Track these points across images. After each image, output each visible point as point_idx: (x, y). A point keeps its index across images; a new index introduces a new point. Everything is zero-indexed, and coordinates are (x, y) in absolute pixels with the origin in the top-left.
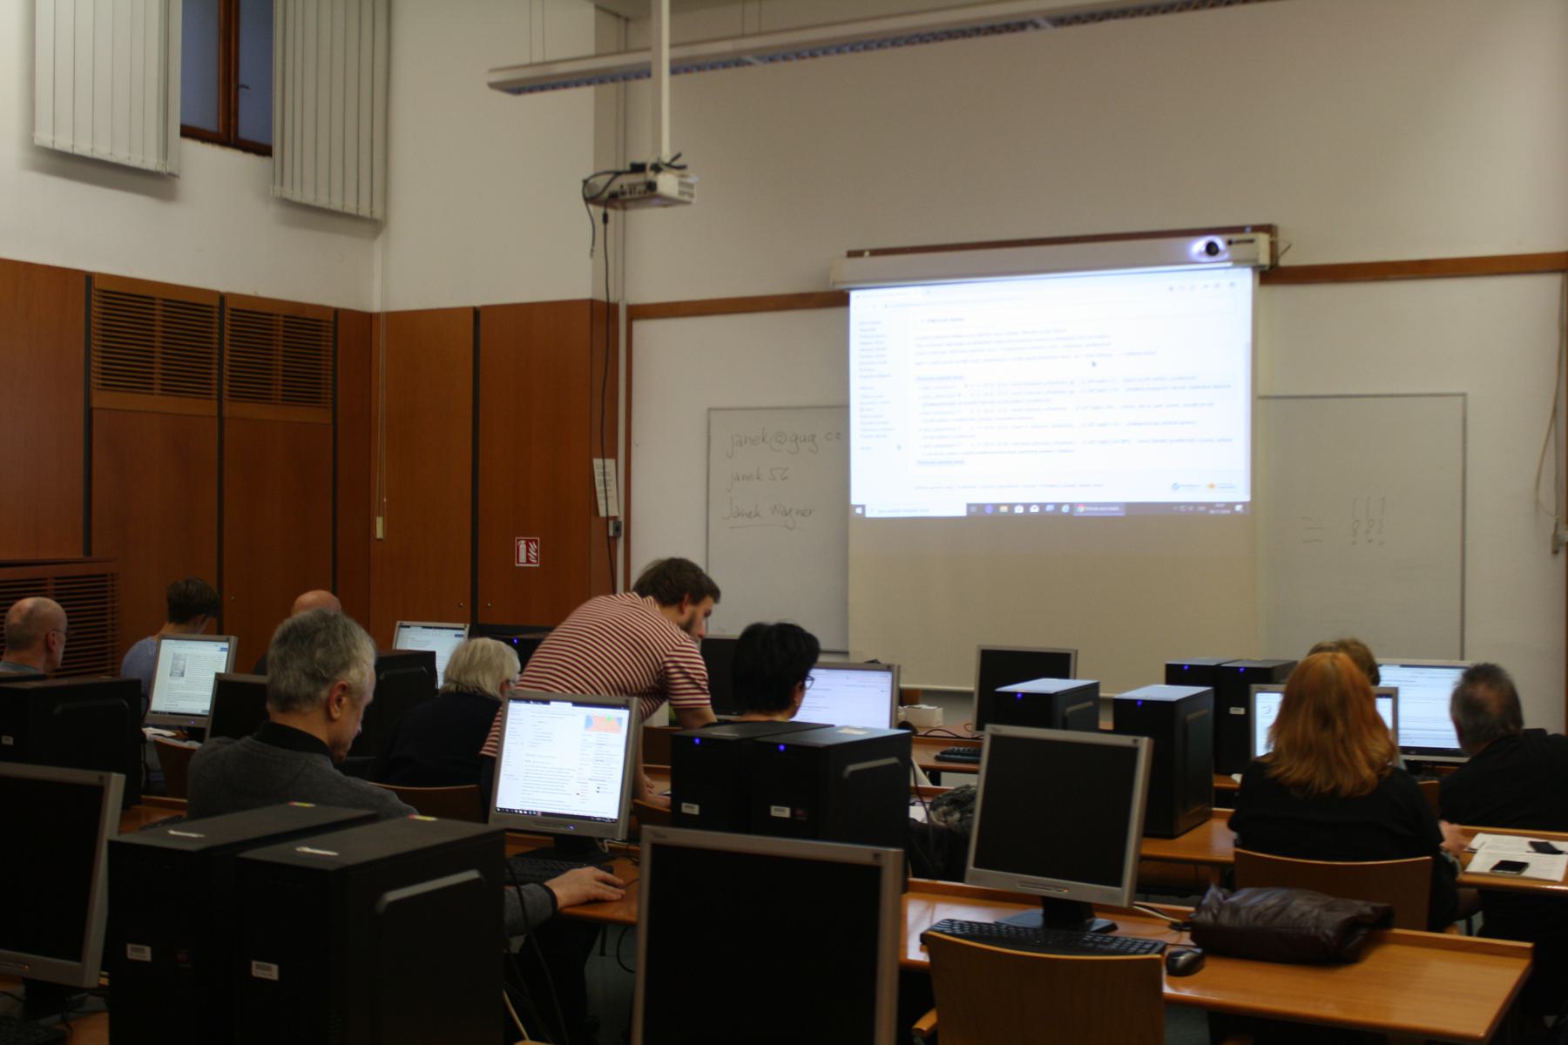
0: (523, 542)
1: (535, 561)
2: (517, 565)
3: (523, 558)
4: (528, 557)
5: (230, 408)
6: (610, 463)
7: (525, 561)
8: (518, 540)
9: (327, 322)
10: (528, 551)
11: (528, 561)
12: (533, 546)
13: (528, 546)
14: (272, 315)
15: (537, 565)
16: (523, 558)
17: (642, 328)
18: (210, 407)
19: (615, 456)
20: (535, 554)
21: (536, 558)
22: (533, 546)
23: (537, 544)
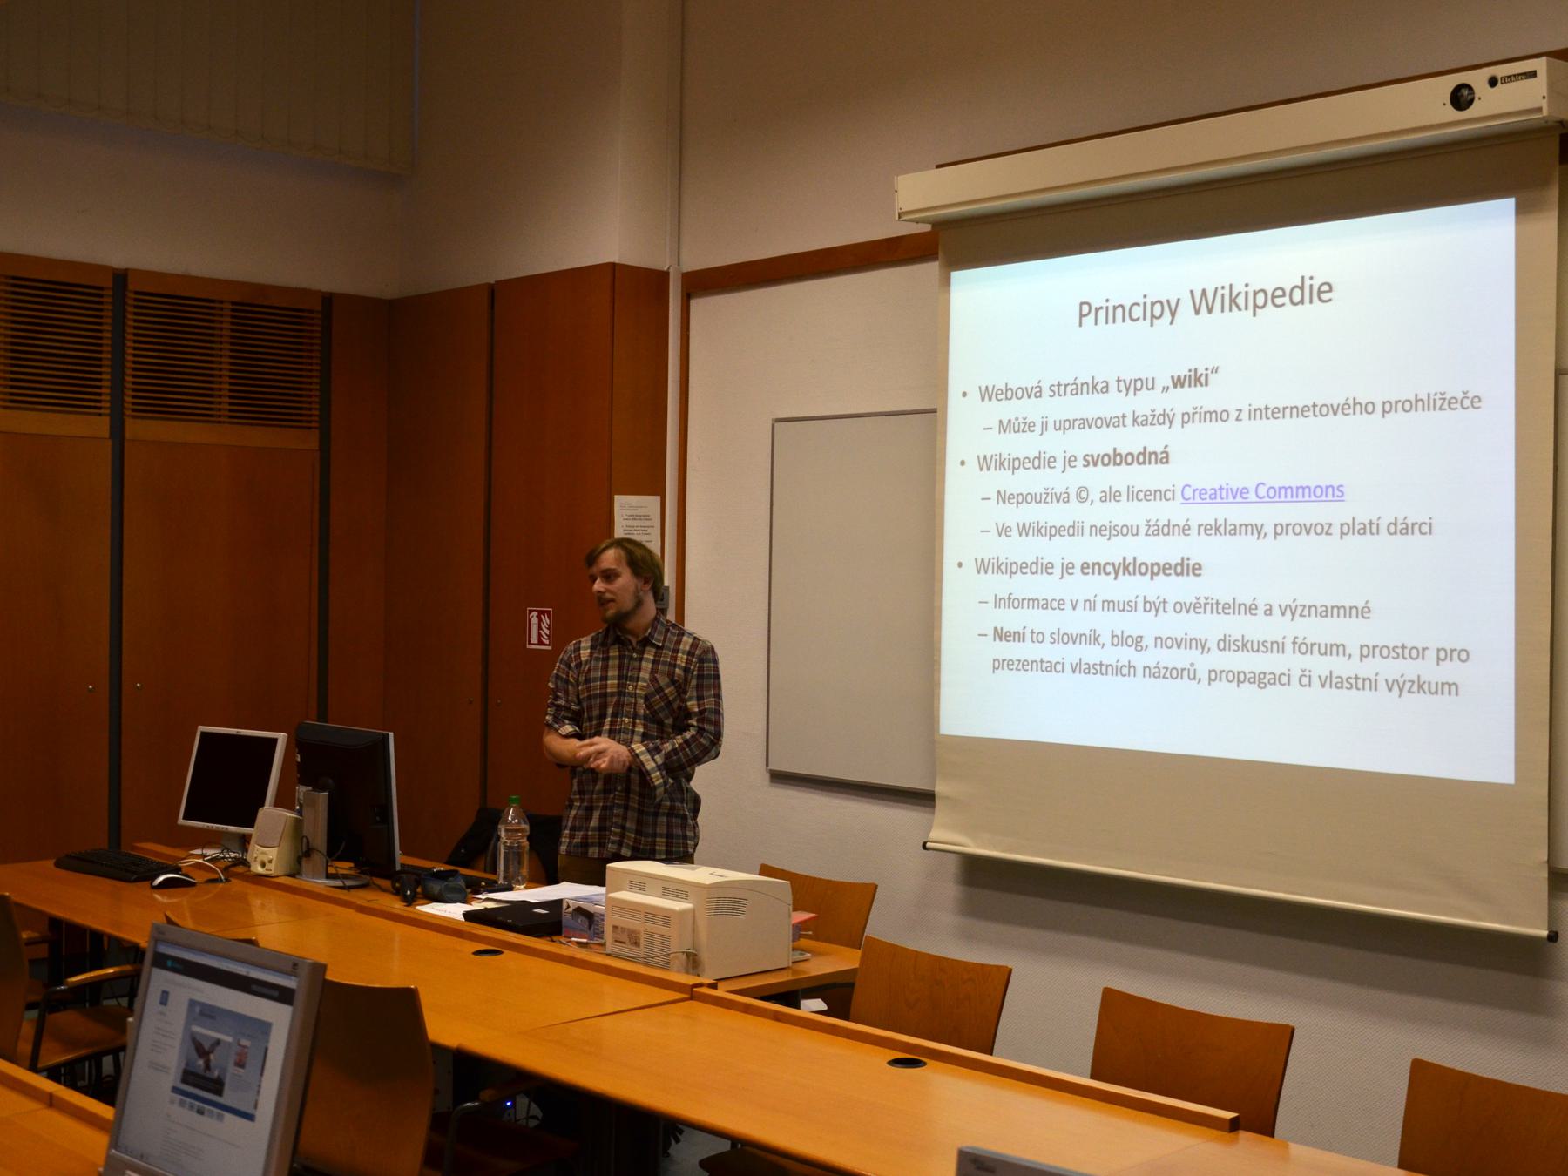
0: (535, 614)
1: (547, 642)
2: (528, 646)
3: (534, 640)
4: (540, 635)
5: (136, 429)
6: (650, 503)
7: (536, 642)
8: (531, 611)
9: (311, 311)
10: (540, 628)
11: (541, 643)
12: (546, 620)
13: (540, 620)
14: (213, 301)
15: (550, 648)
16: (534, 640)
17: (697, 305)
18: (100, 426)
19: (657, 489)
20: (547, 632)
21: (549, 636)
22: (546, 620)
23: (549, 618)
